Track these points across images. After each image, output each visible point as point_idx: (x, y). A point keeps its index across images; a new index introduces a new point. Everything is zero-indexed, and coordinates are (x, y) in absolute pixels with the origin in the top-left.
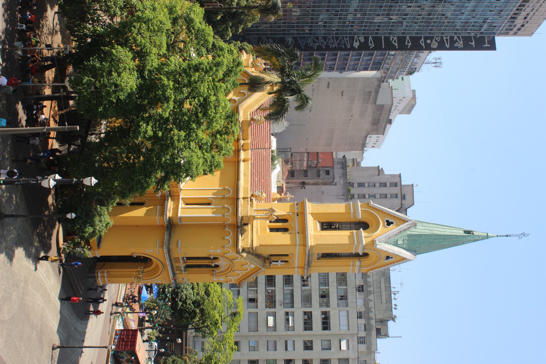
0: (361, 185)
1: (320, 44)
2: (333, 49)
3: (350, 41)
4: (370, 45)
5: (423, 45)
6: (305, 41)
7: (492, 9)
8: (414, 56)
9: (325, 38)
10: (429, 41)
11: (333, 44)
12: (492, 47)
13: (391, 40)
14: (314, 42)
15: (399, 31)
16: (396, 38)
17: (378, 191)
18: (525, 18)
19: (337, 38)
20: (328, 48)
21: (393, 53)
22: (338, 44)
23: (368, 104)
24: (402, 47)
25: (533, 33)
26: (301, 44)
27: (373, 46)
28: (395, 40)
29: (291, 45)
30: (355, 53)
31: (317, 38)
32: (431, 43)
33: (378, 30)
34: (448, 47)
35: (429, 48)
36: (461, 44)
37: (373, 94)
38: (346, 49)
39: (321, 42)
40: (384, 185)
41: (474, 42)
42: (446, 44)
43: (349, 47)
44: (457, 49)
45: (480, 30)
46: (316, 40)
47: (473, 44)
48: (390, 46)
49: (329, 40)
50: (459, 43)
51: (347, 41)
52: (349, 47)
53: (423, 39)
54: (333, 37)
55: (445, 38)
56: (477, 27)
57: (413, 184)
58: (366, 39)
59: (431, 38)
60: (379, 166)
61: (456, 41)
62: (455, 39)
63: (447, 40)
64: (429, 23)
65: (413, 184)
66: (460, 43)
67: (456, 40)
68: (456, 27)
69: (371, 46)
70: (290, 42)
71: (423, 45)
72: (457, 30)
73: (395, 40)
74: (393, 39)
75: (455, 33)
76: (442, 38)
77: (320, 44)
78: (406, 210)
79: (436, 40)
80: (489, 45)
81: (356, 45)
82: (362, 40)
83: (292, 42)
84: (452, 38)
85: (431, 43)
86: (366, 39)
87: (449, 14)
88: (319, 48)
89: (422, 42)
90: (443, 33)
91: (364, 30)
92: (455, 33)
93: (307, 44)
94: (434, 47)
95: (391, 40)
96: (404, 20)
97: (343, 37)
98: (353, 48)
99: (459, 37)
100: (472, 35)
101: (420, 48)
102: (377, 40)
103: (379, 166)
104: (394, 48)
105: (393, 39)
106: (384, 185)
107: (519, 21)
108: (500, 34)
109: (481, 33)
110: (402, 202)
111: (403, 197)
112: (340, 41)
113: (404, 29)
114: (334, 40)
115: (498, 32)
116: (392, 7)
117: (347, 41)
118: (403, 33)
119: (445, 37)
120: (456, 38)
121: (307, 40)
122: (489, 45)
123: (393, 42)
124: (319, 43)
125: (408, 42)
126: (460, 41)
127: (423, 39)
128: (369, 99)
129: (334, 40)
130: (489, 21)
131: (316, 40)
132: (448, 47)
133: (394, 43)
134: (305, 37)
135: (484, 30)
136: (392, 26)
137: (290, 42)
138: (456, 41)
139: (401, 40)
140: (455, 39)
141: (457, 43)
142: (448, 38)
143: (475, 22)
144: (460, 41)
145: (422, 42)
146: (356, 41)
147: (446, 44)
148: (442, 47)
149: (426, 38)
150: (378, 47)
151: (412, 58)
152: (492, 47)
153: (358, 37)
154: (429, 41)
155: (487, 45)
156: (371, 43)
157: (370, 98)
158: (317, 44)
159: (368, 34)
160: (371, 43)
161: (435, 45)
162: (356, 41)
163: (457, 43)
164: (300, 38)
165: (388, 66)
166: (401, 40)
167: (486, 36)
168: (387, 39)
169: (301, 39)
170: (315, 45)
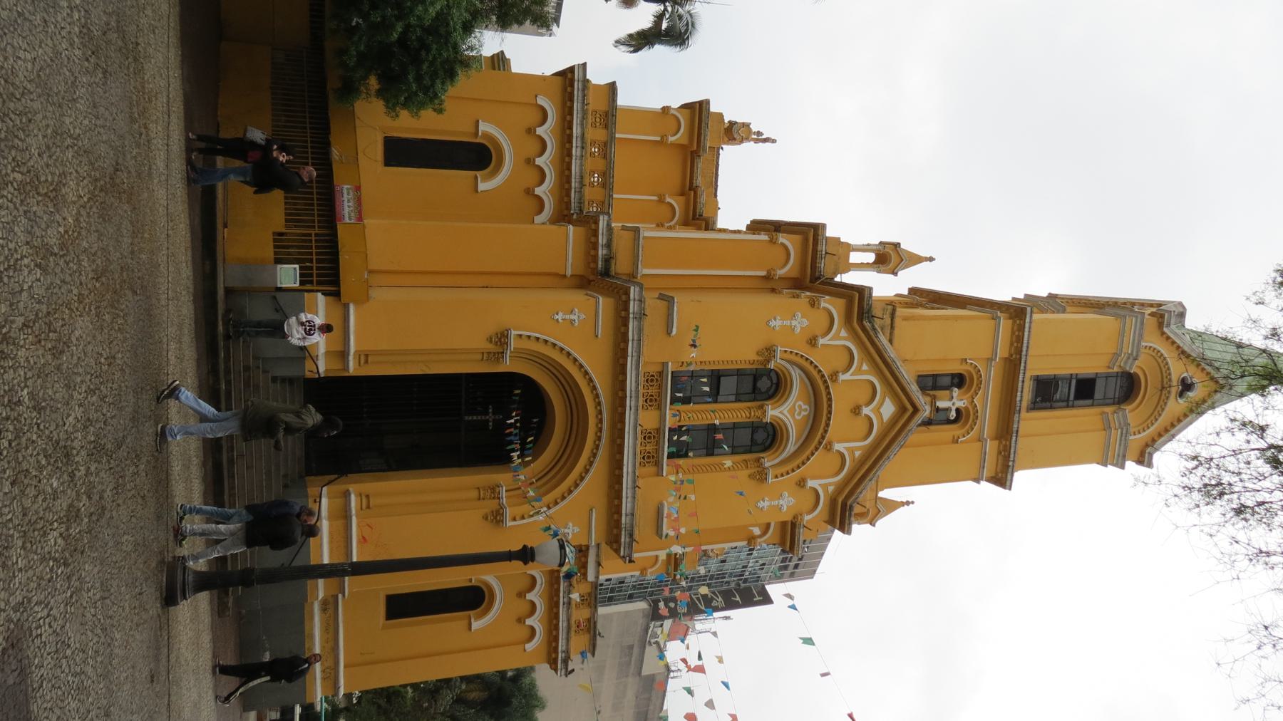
10: (672, 605)
12: (767, 600)
23: (627, 676)
36: (719, 601)
37: (636, 651)
41: (737, 596)
42: (699, 604)
45: (743, 575)
47: (738, 598)
55: (694, 597)
61: (712, 598)
63: (698, 599)
66: (719, 600)
67: (712, 598)
80: (761, 598)
99: (714, 593)
100: (733, 585)
109: (745, 581)
119: (694, 595)
122: (761, 598)
126: (718, 598)
128: (629, 664)
142: (699, 596)
144: (718, 598)
147: (699, 604)
152: (767, 600)
154: (672, 605)
155: (758, 598)
157: (631, 660)
163: (714, 601)
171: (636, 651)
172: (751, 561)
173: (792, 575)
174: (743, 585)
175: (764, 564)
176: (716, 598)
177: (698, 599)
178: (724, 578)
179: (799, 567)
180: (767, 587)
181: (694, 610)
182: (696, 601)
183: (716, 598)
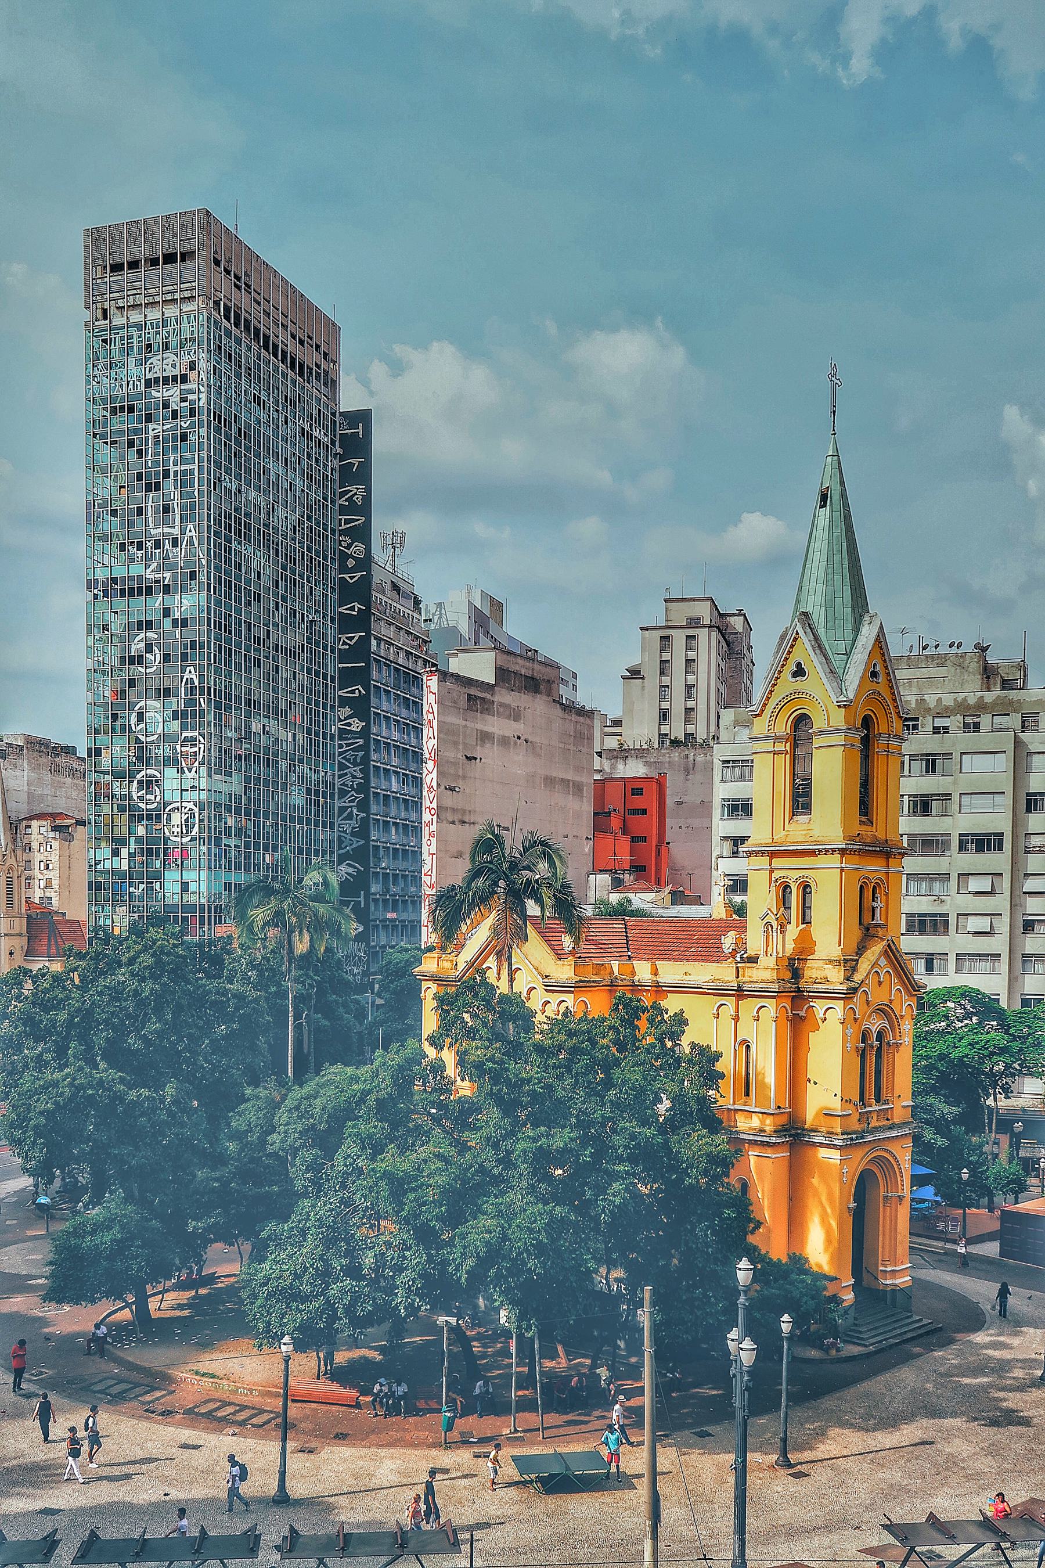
0: (664, 716)
1: (355, 804)
2: (366, 778)
3: (350, 739)
4: (357, 694)
6: (349, 837)
7: (281, 419)
8: (380, 596)
9: (343, 793)
10: (351, 563)
11: (354, 777)
12: (362, 418)
13: (347, 647)
14: (350, 817)
15: (330, 631)
16: (343, 637)
17: (678, 678)
18: (301, 342)
19: (342, 767)
20: (364, 788)
21: (374, 642)
22: (355, 764)
24: (362, 621)
25: (334, 324)
26: (354, 846)
27: (359, 687)
28: (347, 638)
29: (355, 867)
30: (374, 730)
31: (342, 810)
32: (354, 558)
33: (325, 678)
35: (366, 563)
36: (357, 491)
38: (365, 747)
39: (349, 802)
40: (664, 667)
42: (359, 522)
43: (361, 741)
44: (367, 499)
45: (327, 446)
46: (345, 814)
47: (356, 461)
48: (361, 650)
49: (347, 786)
50: (356, 494)
51: (348, 745)
52: (361, 741)
54: (340, 776)
55: (343, 527)
56: (319, 453)
57: (665, 600)
58: (344, 702)
59: (344, 557)
60: (624, 678)
62: (347, 503)
63: (347, 522)
64: (311, 563)
65: (665, 600)
69: (360, 691)
70: (350, 870)
72: (325, 499)
73: (347, 638)
74: (344, 643)
75: (333, 502)
76: (342, 533)
77: (355, 804)
78: (721, 615)
79: (348, 547)
81: (357, 725)
82: (347, 711)
83: (348, 865)
85: (354, 558)
86: (344, 702)
87: (293, 518)
88: (363, 806)
89: (352, 578)
90: (333, 531)
91: (325, 707)
92: (333, 502)
93: (353, 834)
95: (347, 647)
96: (306, 618)
97: (340, 754)
98: (365, 733)
100: (336, 463)
101: (367, 580)
102: (347, 678)
103: (624, 678)
104: (365, 641)
105: (344, 643)
106: (664, 667)
107: (310, 358)
108: (334, 397)
109: (333, 443)
110: (704, 627)
111: (694, 622)
112: (348, 760)
113: (324, 617)
114: (346, 774)
115: (331, 404)
116: (277, 645)
117: (348, 745)
118: (333, 620)
119: (341, 526)
121: (345, 832)
123: (352, 643)
124: (351, 807)
125: (352, 609)
129: (346, 774)
130: (307, 427)
131: (345, 814)
133: (354, 641)
134: (339, 837)
135: (327, 436)
136: (317, 644)
137: (350, 870)
139: (346, 624)
140: (347, 503)
143: (309, 456)
145: (352, 578)
146: (349, 725)
147: (359, 522)
148: (362, 534)
149: (343, 569)
150: (362, 676)
151: (384, 599)
153: (340, 720)
154: (351, 563)
155: (360, 430)
156: (353, 692)
158: (355, 811)
159: (334, 698)
160: (353, 692)
161: (358, 549)
162: (349, 725)
164: (340, 848)
165: (401, 655)
166: (346, 624)
167: (338, 432)
168: (344, 656)
169: (343, 846)
170: (357, 815)
176: (349, 495)
177: (347, 522)
178: (327, 476)
183: (349, 495)
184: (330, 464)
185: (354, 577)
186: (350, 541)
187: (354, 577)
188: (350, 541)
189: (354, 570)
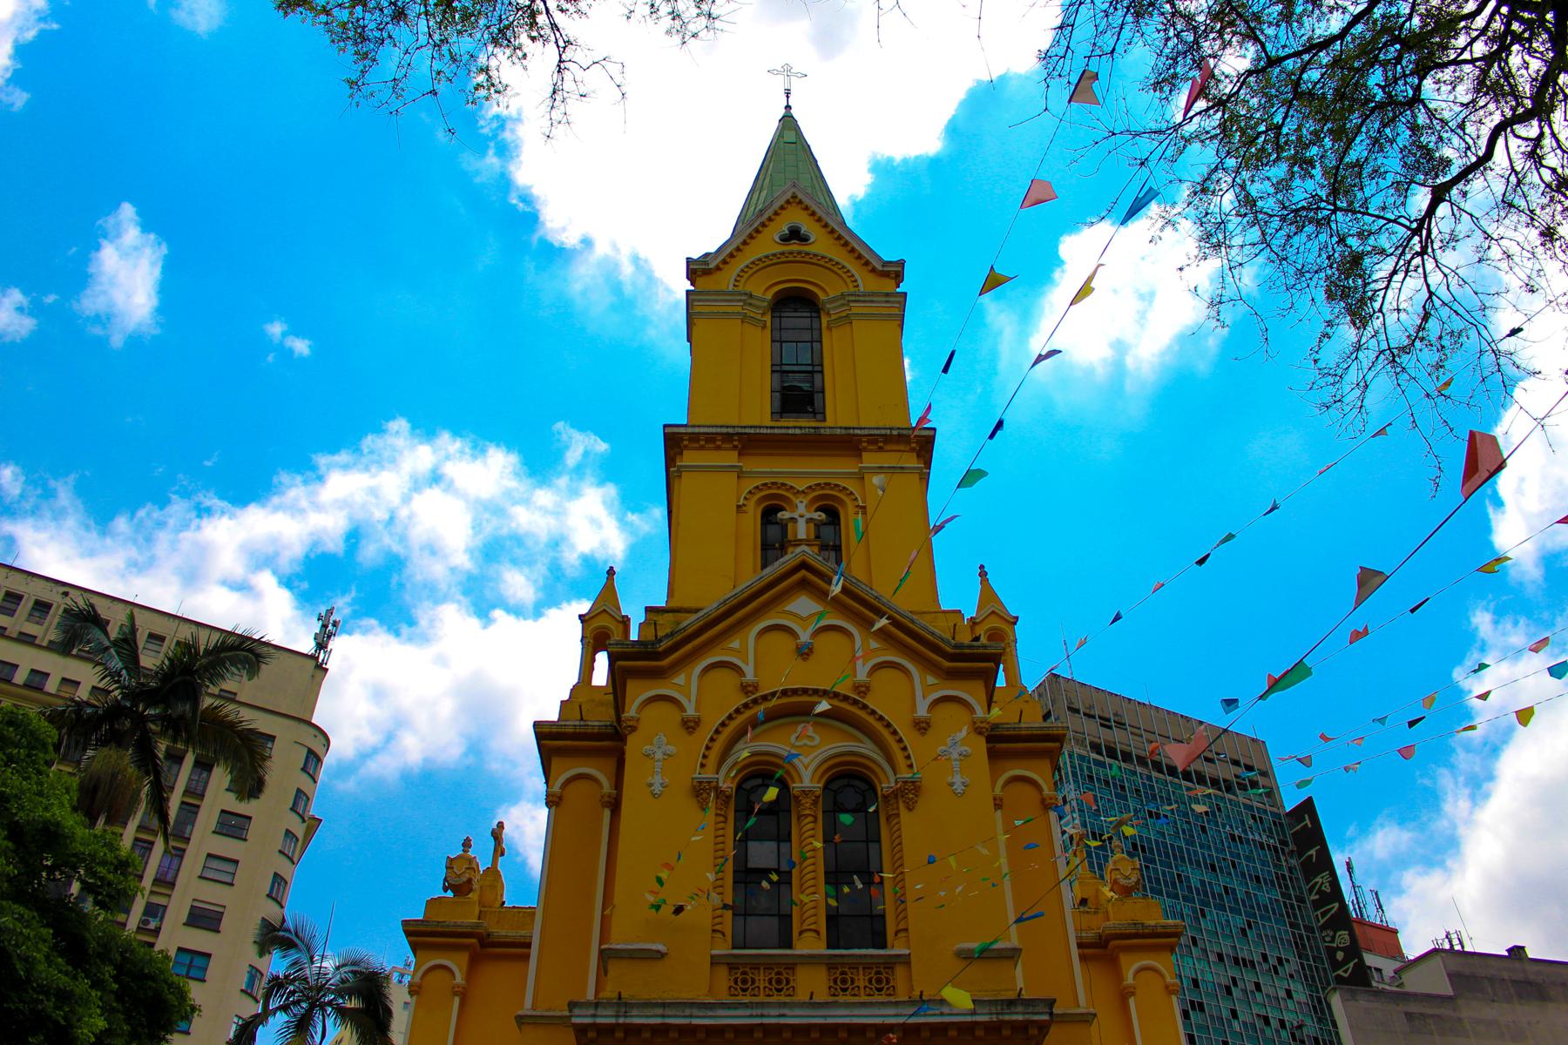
5: (1351, 964)
10: (1340, 956)
12: (1307, 807)
23: (1460, 1020)
32: (1342, 949)
34: (1336, 905)
36: (1321, 880)
37: (1414, 1008)
41: (1310, 853)
42: (1333, 911)
45: (1275, 848)
47: (1313, 852)
50: (1323, 883)
53: (1340, 972)
55: (1322, 922)
59: (1331, 952)
63: (1323, 914)
68: (1277, 900)
71: (1351, 964)
76: (1323, 928)
79: (1333, 941)
80: (1306, 816)
84: (1317, 905)
85: (1342, 949)
94: (1347, 937)
99: (1311, 890)
100: (1293, 862)
109: (1284, 843)
120: (1314, 897)
122: (1306, 816)
126: (1316, 883)
127: (1340, 972)
132: (1336, 905)
138: (1320, 892)
141: (1323, 888)
142: (1318, 913)
144: (1316, 883)
145: (1345, 971)
147: (1333, 911)
152: (1307, 807)
154: (1340, 956)
155: (1308, 821)
157: (1433, 1016)
161: (1343, 937)
163: (1323, 888)
171: (1414, 1008)
172: (1251, 837)
173: (1264, 774)
174: (1292, 847)
175: (1254, 817)
176: (1317, 887)
177: (1323, 914)
178: (1283, 876)
179: (1249, 763)
180: (1288, 810)
181: (1342, 919)
182: (1328, 916)
183: (1317, 887)
184: (1284, 864)
185: (1348, 969)
186: (1331, 933)
187: (1348, 969)
188: (1331, 933)
189: (1346, 961)
